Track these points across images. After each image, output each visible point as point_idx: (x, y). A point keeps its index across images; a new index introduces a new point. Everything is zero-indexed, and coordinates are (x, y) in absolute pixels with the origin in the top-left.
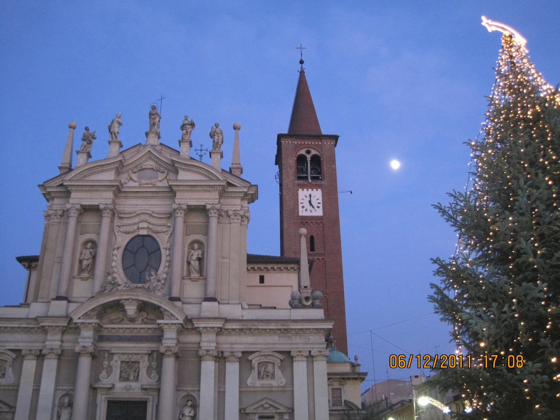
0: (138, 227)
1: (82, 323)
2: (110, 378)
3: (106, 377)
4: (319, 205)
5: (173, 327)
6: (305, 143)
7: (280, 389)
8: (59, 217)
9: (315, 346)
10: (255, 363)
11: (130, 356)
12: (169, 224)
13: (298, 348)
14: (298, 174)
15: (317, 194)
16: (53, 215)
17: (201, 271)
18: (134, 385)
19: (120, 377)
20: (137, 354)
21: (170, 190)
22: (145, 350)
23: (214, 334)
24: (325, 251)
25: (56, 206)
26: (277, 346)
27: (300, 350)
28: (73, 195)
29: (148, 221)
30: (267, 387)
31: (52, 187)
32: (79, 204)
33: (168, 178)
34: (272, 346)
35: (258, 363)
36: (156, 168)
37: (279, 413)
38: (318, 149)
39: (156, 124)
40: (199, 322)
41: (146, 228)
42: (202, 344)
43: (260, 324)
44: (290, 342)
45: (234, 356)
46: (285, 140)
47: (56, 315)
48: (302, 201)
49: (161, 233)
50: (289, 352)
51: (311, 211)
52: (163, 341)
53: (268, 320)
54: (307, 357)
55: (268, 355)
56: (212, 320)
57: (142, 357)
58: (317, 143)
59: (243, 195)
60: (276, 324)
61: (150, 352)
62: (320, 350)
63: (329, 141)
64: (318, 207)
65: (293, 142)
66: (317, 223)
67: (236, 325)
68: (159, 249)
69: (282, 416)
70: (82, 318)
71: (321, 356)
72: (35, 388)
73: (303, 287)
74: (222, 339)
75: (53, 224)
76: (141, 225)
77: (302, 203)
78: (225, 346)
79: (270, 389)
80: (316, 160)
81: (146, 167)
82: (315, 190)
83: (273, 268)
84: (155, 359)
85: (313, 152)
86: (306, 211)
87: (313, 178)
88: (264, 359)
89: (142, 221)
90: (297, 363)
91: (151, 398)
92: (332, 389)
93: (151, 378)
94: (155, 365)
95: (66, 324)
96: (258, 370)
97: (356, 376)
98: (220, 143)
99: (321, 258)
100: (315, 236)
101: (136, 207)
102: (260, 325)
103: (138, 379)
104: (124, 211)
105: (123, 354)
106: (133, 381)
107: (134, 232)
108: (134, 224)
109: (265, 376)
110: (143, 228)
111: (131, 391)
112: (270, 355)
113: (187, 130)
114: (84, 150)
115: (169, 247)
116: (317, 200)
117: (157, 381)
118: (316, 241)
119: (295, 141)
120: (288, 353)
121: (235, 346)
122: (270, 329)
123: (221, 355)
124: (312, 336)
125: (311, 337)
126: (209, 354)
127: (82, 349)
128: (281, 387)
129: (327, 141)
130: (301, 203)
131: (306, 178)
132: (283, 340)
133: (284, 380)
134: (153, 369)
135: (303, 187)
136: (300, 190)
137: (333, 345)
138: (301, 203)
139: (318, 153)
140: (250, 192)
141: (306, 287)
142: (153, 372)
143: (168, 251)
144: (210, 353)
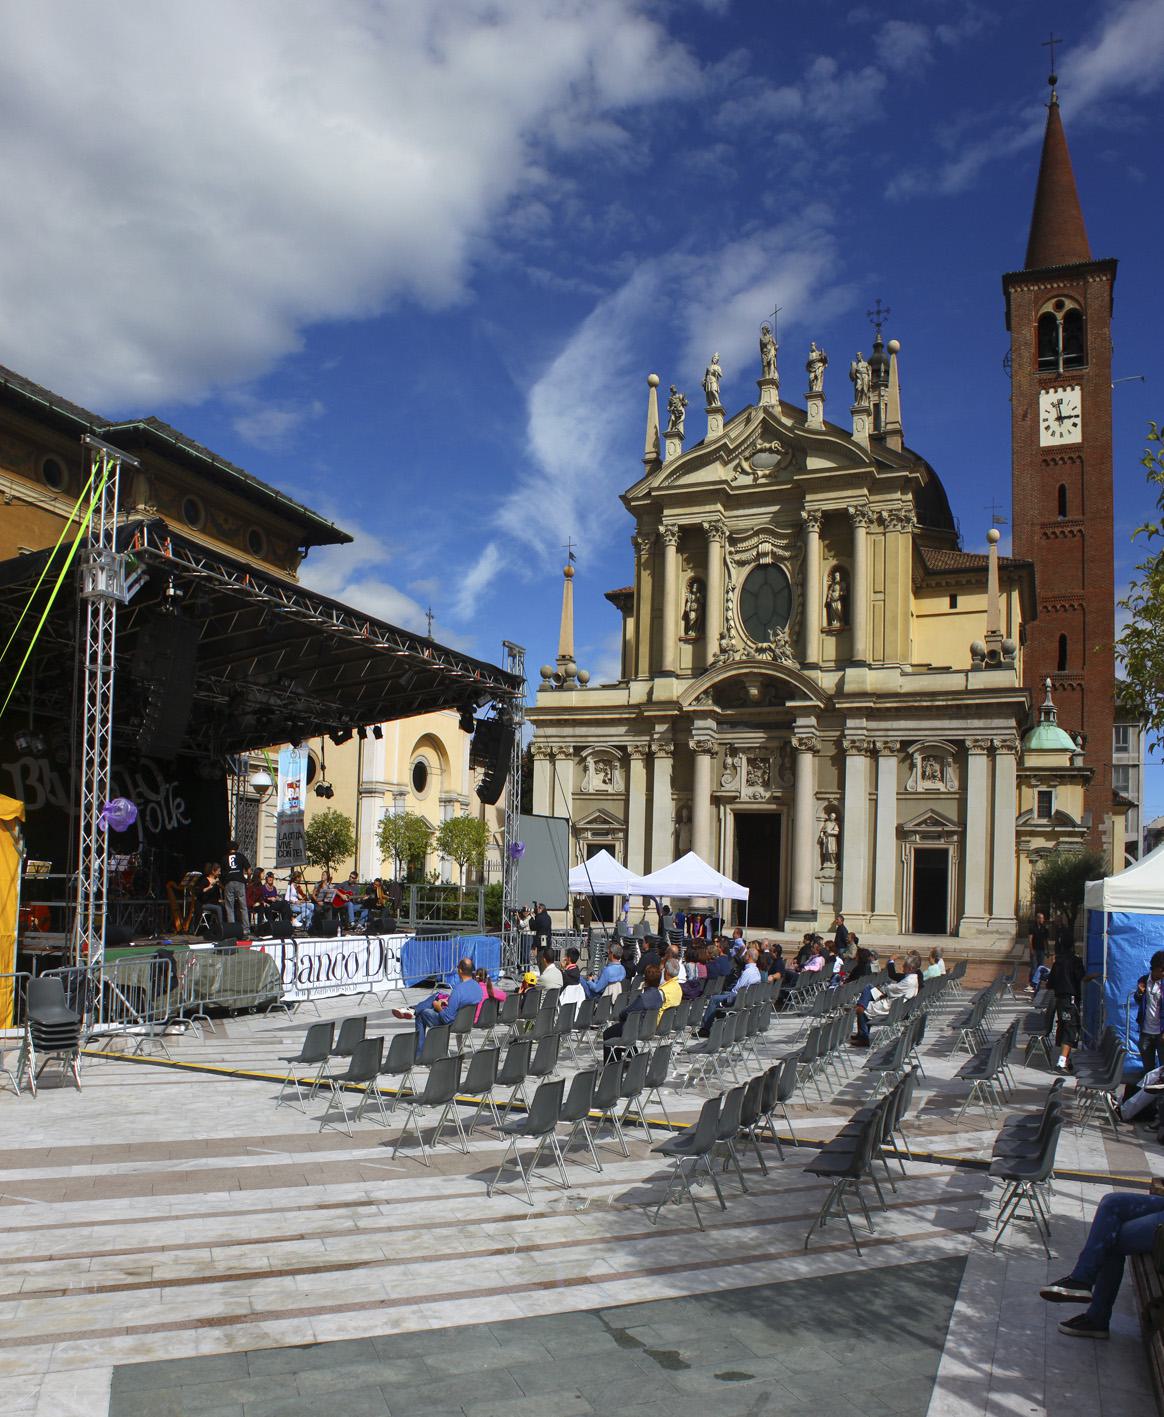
1: (694, 711)
9: (999, 732)
10: (918, 758)
14: (1040, 357)
15: (1072, 398)
24: (1083, 514)
27: (979, 738)
35: (923, 759)
42: (847, 732)
48: (1046, 415)
50: (963, 741)
51: (1061, 435)
52: (796, 730)
54: (988, 749)
64: (1075, 425)
70: (695, 703)
80: (1074, 319)
85: (1069, 305)
87: (1067, 362)
99: (1075, 529)
120: (960, 743)
123: (872, 746)
131: (1055, 364)
135: (1047, 385)
136: (1043, 392)
137: (1052, 719)
138: (1046, 420)
139: (1078, 307)
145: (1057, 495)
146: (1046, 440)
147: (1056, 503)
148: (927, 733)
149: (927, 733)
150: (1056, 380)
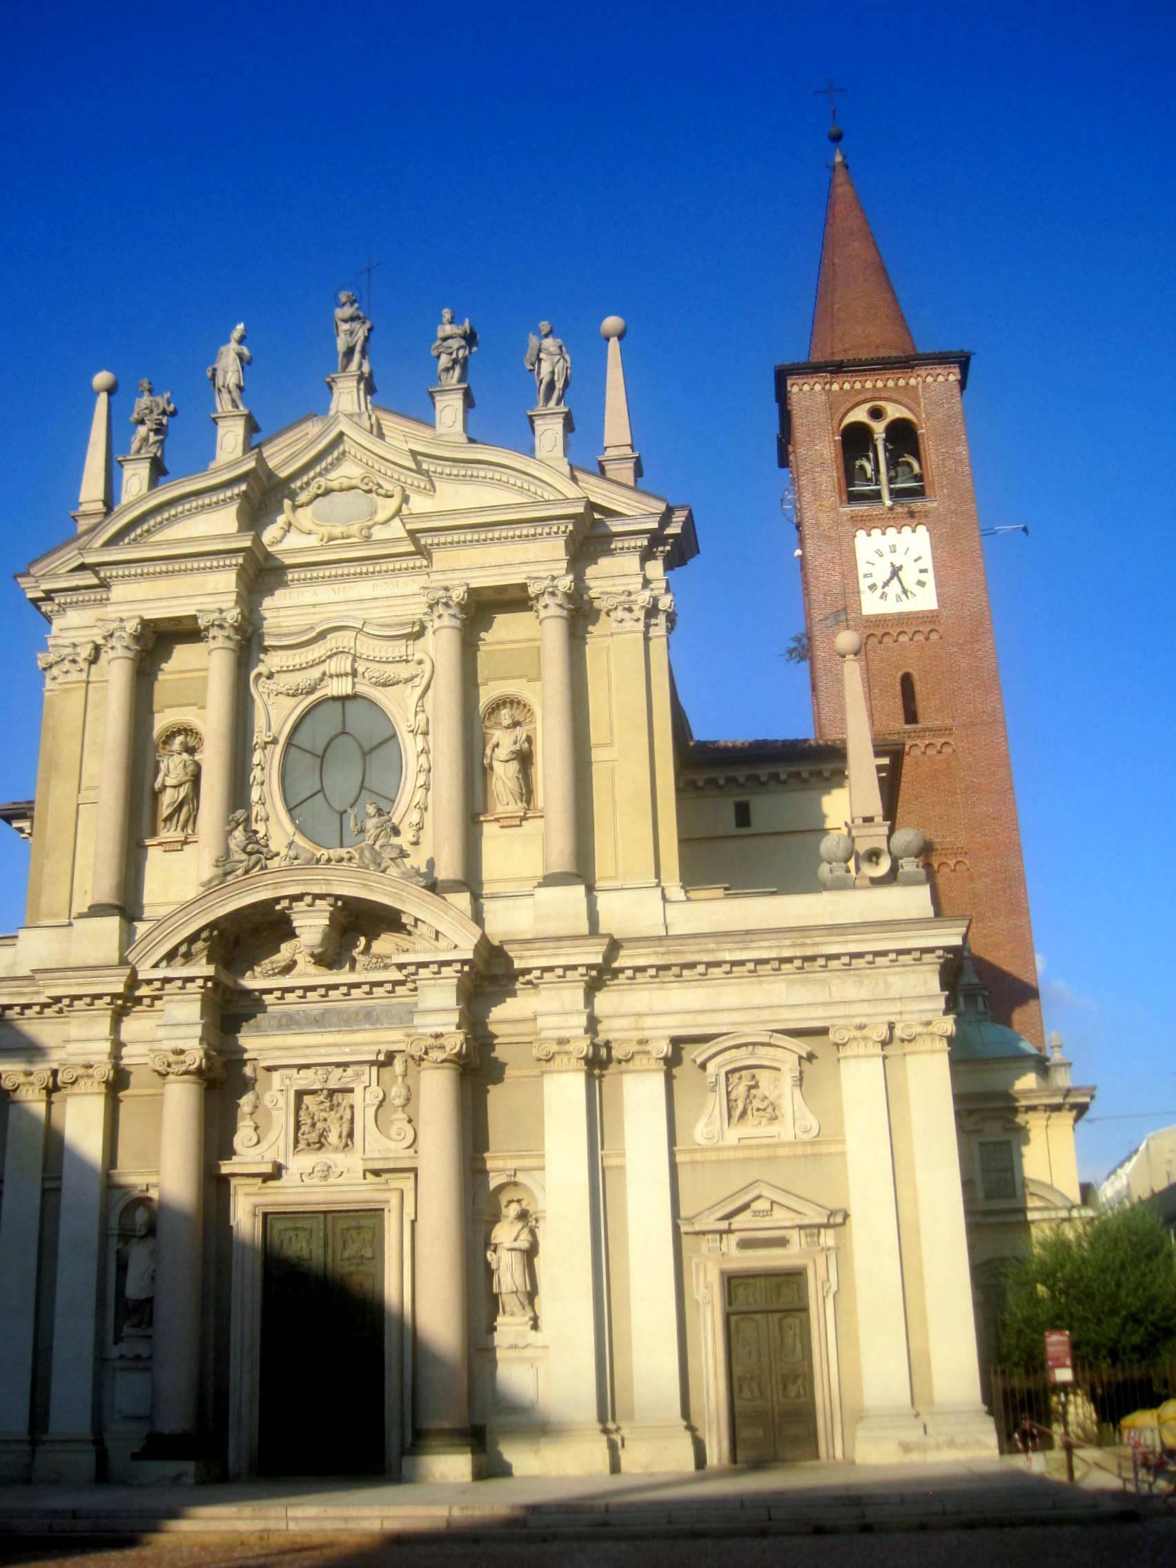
0: (324, 674)
2: (264, 1144)
3: (255, 1140)
4: (923, 577)
5: (446, 971)
6: (863, 387)
7: (800, 1151)
8: (84, 666)
11: (321, 1070)
12: (417, 657)
13: (853, 1016)
16: (66, 662)
17: (527, 792)
18: (339, 1160)
19: (297, 1141)
20: (345, 1065)
21: (412, 548)
22: (370, 1053)
23: (578, 987)
25: (72, 633)
26: (785, 1014)
27: (863, 1020)
28: (118, 592)
29: (352, 652)
30: (758, 1147)
31: (56, 576)
32: (134, 617)
33: (405, 511)
34: (766, 1015)
35: (727, 1073)
36: (367, 484)
37: (801, 1227)
38: (905, 400)
39: (358, 348)
40: (525, 953)
41: (346, 675)
42: (541, 1022)
43: (723, 946)
44: (827, 999)
45: (647, 1053)
46: (801, 382)
47: (91, 962)
49: (393, 685)
50: (824, 1031)
52: (417, 1020)
53: (748, 932)
54: (884, 1044)
55: (754, 1044)
56: (569, 943)
57: (358, 1075)
58: (902, 382)
59: (645, 543)
60: (774, 943)
61: (381, 1057)
62: (925, 1017)
63: (939, 371)
64: (921, 583)
65: (827, 387)
66: (919, 631)
67: (647, 955)
68: (394, 736)
69: (812, 1235)
70: (164, 963)
71: (929, 1039)
72: (48, 1185)
73: (859, 821)
74: (605, 1001)
75: (67, 690)
76: (333, 666)
77: (871, 575)
78: (616, 1023)
79: (771, 1152)
81: (335, 485)
82: (907, 530)
83: (775, 777)
84: (400, 1079)
85: (893, 412)
86: (881, 597)
87: (896, 494)
88: (742, 1057)
89: (336, 654)
90: (852, 1061)
91: (394, 1199)
92: (981, 1144)
93: (392, 1140)
94: (400, 1097)
95: (120, 989)
96: (728, 1093)
97: (1058, 1100)
98: (559, 385)
100: (916, 676)
101: (313, 610)
102: (724, 950)
103: (353, 1143)
104: (280, 627)
105: (301, 1067)
106: (336, 1149)
107: (312, 690)
108: (312, 666)
109: (749, 1111)
110: (339, 676)
111: (331, 1180)
112: (763, 1044)
113: (451, 354)
114: (143, 451)
115: (423, 724)
116: (915, 561)
117: (409, 1147)
118: (919, 688)
119: (831, 384)
121: (648, 1022)
122: (759, 962)
123: (604, 1052)
124: (895, 974)
125: (891, 979)
126: (567, 1053)
127: (172, 1058)
128: (805, 1143)
129: (935, 372)
130: (865, 576)
131: (877, 496)
132: (802, 994)
133: (813, 1122)
134: (395, 1108)
135: (866, 523)
136: (861, 534)
138: (865, 576)
140: (669, 531)
141: (868, 820)
142: (395, 1116)
143: (420, 738)
144: (568, 1047)
145: (899, 688)
146: (871, 605)
147: (899, 701)
148: (736, 1017)
149: (736, 1017)
150: (879, 518)
